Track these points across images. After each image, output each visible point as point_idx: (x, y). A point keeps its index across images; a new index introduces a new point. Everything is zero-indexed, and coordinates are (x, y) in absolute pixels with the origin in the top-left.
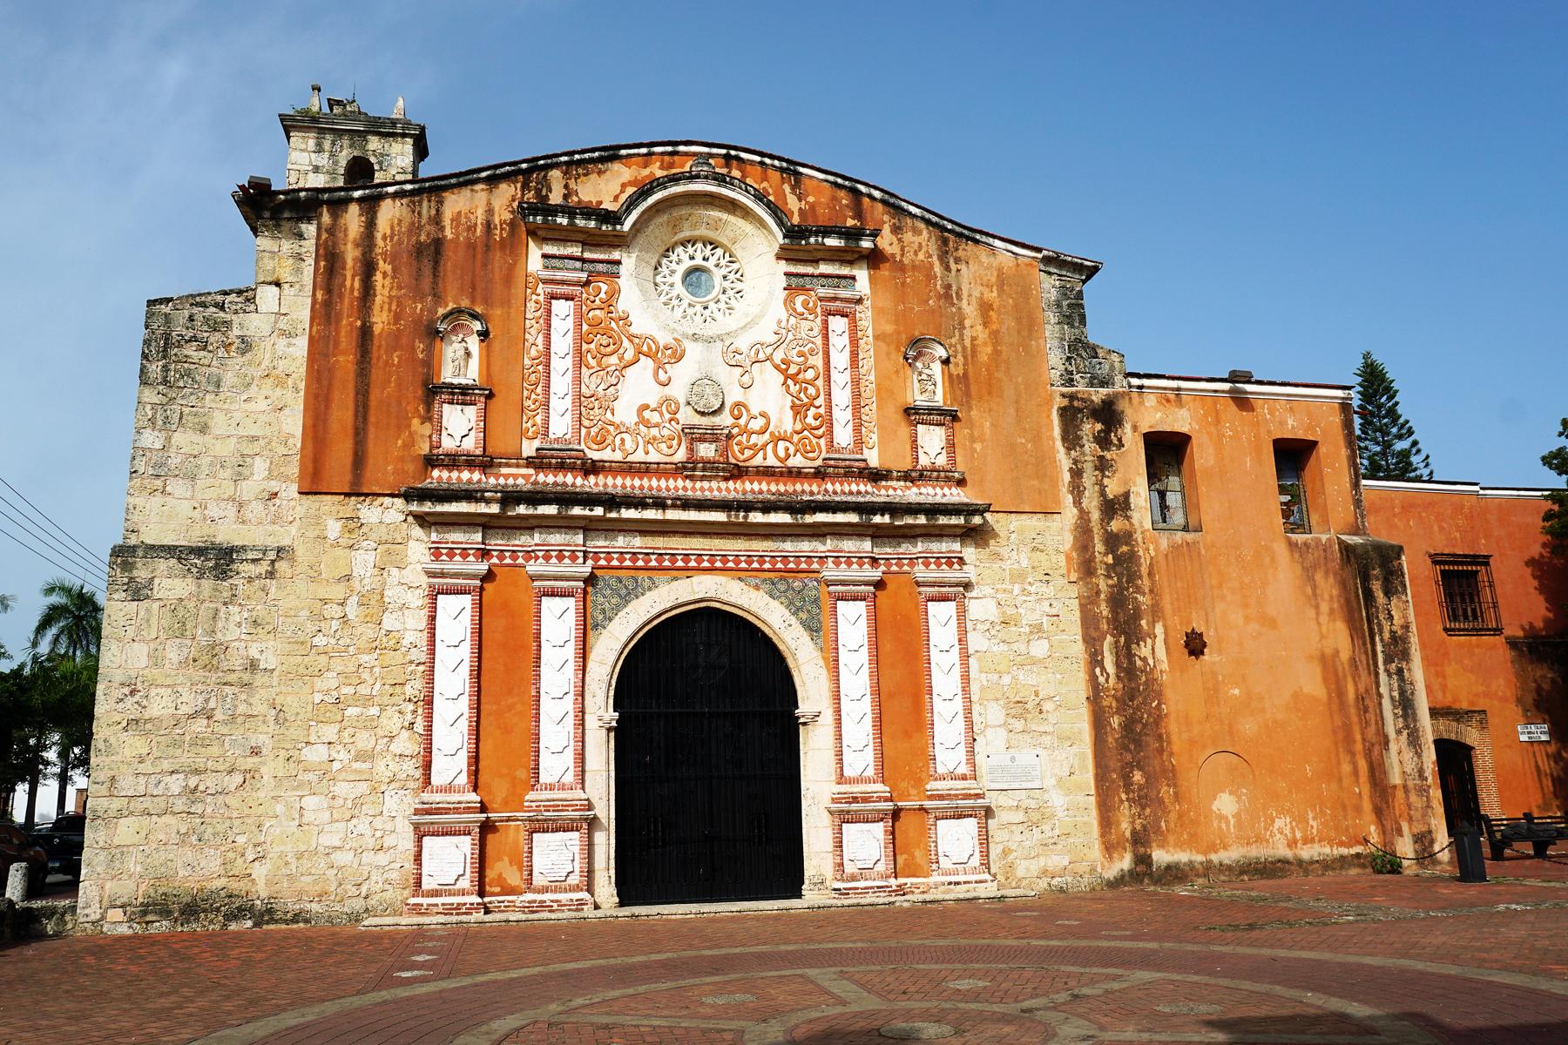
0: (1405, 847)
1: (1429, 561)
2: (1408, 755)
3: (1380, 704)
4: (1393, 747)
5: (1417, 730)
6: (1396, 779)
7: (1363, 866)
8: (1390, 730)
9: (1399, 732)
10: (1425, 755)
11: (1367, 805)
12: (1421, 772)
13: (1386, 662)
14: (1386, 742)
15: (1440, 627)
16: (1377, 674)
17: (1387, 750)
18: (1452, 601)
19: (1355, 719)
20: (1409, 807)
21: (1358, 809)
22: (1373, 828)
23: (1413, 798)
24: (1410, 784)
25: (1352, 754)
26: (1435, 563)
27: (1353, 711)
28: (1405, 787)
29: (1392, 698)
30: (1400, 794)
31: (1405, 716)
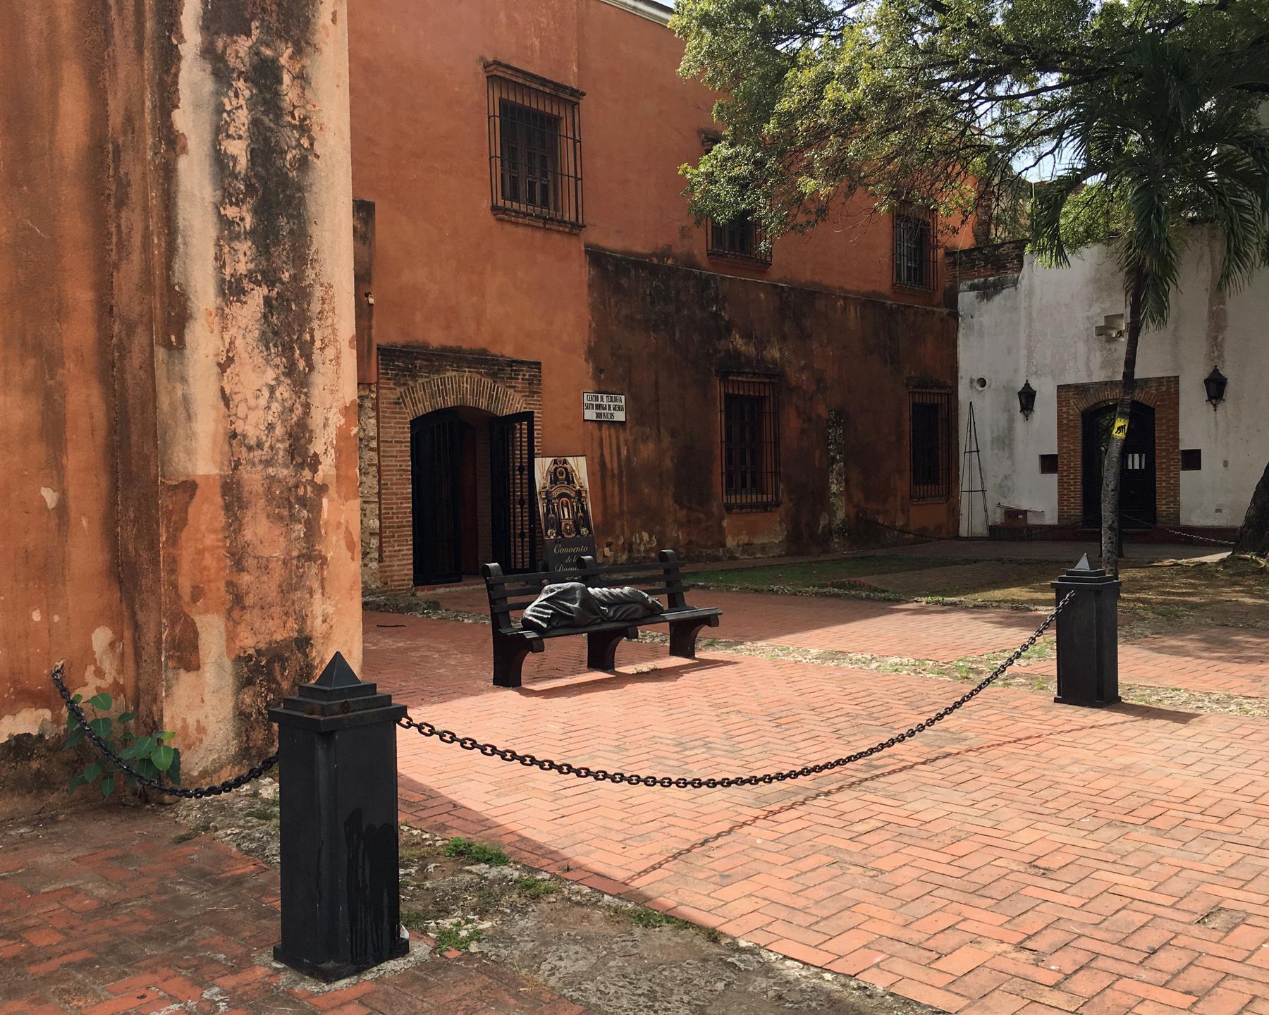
0: (203, 712)
1: (482, 77)
2: (257, 376)
3: (168, 173)
4: (203, 341)
5: (301, 293)
6: (199, 455)
7: (41, 783)
8: (200, 275)
9: (232, 290)
10: (320, 380)
11: (85, 553)
12: (298, 437)
13: (209, 24)
14: (175, 317)
15: (486, 204)
16: (169, 57)
17: (177, 347)
18: (514, 166)
19: (74, 226)
20: (238, 559)
21: (44, 571)
22: (101, 638)
23: (260, 530)
24: (253, 478)
25: (50, 360)
26: (491, 79)
27: (70, 194)
28: (232, 493)
29: (221, 161)
30: (206, 515)
31: (264, 237)
